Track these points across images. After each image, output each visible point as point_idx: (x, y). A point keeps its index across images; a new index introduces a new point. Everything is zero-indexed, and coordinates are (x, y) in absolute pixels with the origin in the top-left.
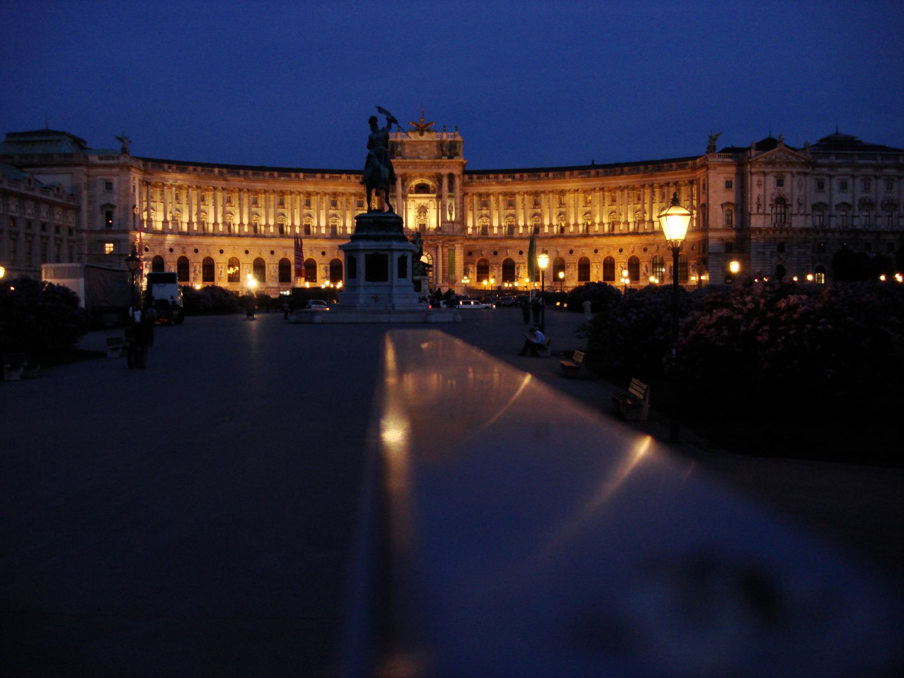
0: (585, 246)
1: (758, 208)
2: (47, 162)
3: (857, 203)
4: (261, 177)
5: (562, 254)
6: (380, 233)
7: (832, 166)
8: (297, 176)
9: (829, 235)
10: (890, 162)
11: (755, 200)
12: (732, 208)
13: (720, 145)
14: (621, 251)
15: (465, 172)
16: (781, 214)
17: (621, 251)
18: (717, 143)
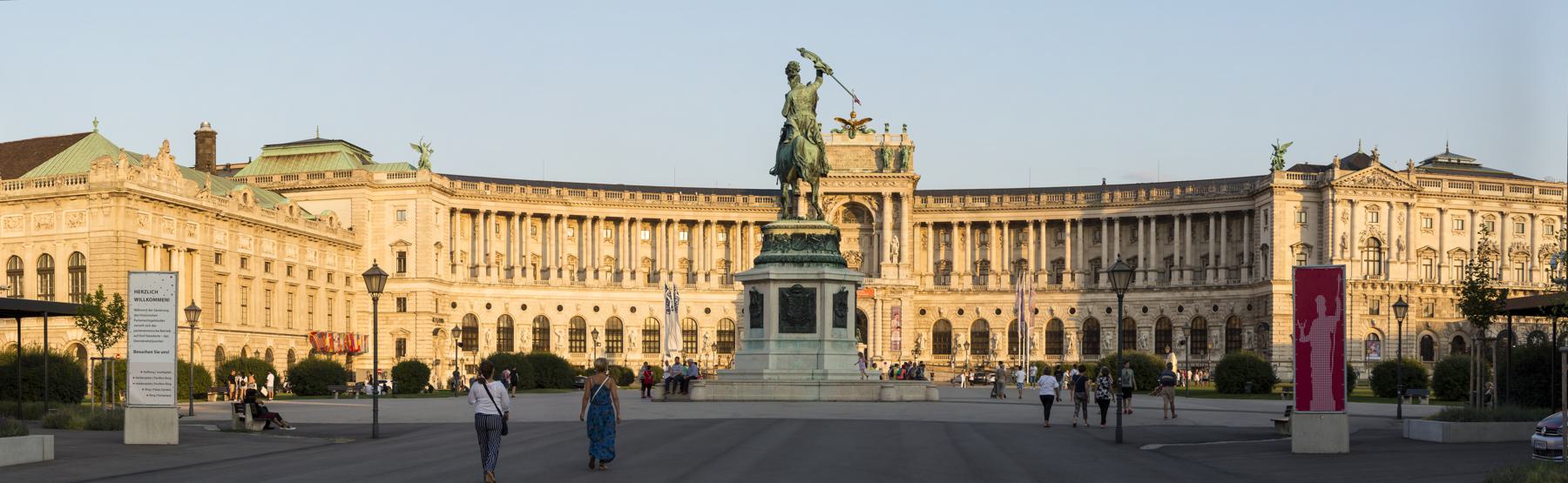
0: (1094, 302)
2: (318, 182)
4: (617, 200)
5: (1058, 314)
8: (670, 198)
9: (1439, 292)
11: (1338, 241)
13: (1290, 160)
14: (1145, 310)
15: (916, 193)
17: (1145, 310)
18: (1284, 156)
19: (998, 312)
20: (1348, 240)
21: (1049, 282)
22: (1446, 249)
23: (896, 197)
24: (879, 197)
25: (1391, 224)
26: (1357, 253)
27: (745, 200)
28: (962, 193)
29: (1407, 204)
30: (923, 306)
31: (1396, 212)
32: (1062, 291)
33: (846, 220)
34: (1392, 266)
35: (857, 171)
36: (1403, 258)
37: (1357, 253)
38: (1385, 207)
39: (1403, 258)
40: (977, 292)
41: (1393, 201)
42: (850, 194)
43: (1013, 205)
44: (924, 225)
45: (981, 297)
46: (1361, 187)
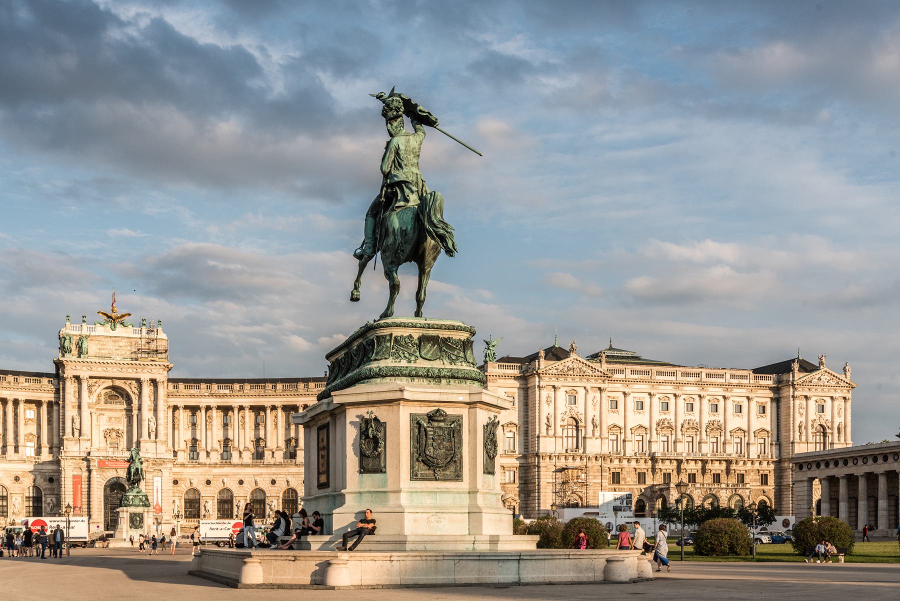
1: (547, 429)
3: (654, 426)
6: (437, 365)
7: (625, 381)
9: (625, 462)
10: (692, 379)
11: (544, 421)
12: (514, 429)
16: (572, 437)
19: (241, 482)
20: (552, 420)
21: (285, 458)
22: (629, 427)
23: (154, 382)
24: (138, 381)
25: (589, 405)
26: (559, 430)
27: (16, 380)
28: (209, 381)
29: (600, 389)
30: (176, 477)
31: (591, 394)
32: (296, 465)
34: (588, 441)
36: (597, 434)
37: (559, 430)
38: (582, 392)
39: (597, 434)
40: (222, 465)
41: (588, 386)
42: (111, 378)
43: (253, 392)
44: (175, 408)
45: (227, 470)
46: (563, 374)
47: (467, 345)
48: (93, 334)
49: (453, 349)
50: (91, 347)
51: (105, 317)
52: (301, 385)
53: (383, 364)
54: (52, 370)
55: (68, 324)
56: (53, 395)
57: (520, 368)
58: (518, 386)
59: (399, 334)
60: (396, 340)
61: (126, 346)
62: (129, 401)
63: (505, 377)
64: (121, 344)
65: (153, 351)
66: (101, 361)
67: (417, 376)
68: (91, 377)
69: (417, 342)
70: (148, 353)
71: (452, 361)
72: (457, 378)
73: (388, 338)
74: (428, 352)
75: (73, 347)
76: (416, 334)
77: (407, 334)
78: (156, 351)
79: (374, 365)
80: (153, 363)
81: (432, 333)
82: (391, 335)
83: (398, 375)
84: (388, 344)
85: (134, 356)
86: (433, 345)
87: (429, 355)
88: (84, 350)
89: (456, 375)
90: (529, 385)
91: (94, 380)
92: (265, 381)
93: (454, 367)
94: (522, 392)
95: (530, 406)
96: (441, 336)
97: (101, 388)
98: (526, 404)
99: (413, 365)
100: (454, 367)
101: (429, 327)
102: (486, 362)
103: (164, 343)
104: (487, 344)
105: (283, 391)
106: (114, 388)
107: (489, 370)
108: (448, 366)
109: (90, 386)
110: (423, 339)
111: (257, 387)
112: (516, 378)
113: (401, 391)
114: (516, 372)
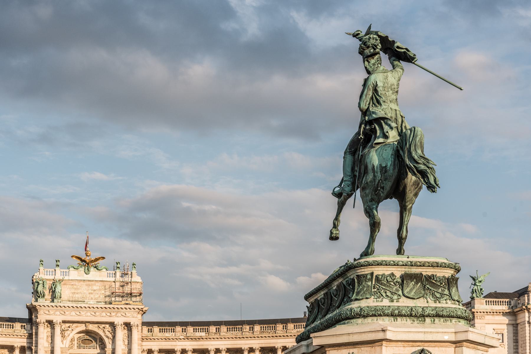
6: (421, 303)
23: (128, 326)
24: (112, 325)
33: (79, 347)
35: (92, 303)
43: (230, 334)
47: (451, 282)
48: (66, 278)
49: (438, 287)
50: (64, 291)
51: (79, 261)
52: (280, 327)
53: (364, 304)
54: (26, 316)
55: (41, 268)
56: (25, 340)
57: (509, 303)
58: (507, 321)
59: (381, 273)
60: (378, 279)
61: (100, 290)
62: (103, 346)
63: (493, 313)
64: (95, 288)
65: (127, 294)
66: (74, 305)
67: (400, 315)
68: (64, 322)
69: (399, 280)
70: (123, 297)
71: (437, 299)
72: (442, 316)
73: (369, 277)
74: (411, 290)
75: (47, 292)
76: (398, 272)
77: (389, 273)
78: (131, 294)
79: (355, 306)
80: (127, 306)
81: (415, 270)
82: (372, 274)
83: (380, 315)
84: (370, 283)
85: (107, 299)
86: (417, 283)
87: (413, 293)
88: (58, 294)
89: (441, 313)
90: (519, 321)
91: (68, 325)
92: (242, 323)
93: (438, 305)
94: (511, 328)
95: (520, 342)
96: (424, 274)
97: (74, 332)
98: (516, 341)
99: (395, 304)
100: (438, 305)
101: (412, 264)
102: (473, 298)
103: (138, 286)
104: (474, 279)
105: (261, 332)
106: (87, 332)
107: (476, 306)
108: (432, 304)
109: (63, 331)
110: (406, 277)
111: (234, 329)
112: (505, 314)
113: (384, 331)
114: (505, 308)
